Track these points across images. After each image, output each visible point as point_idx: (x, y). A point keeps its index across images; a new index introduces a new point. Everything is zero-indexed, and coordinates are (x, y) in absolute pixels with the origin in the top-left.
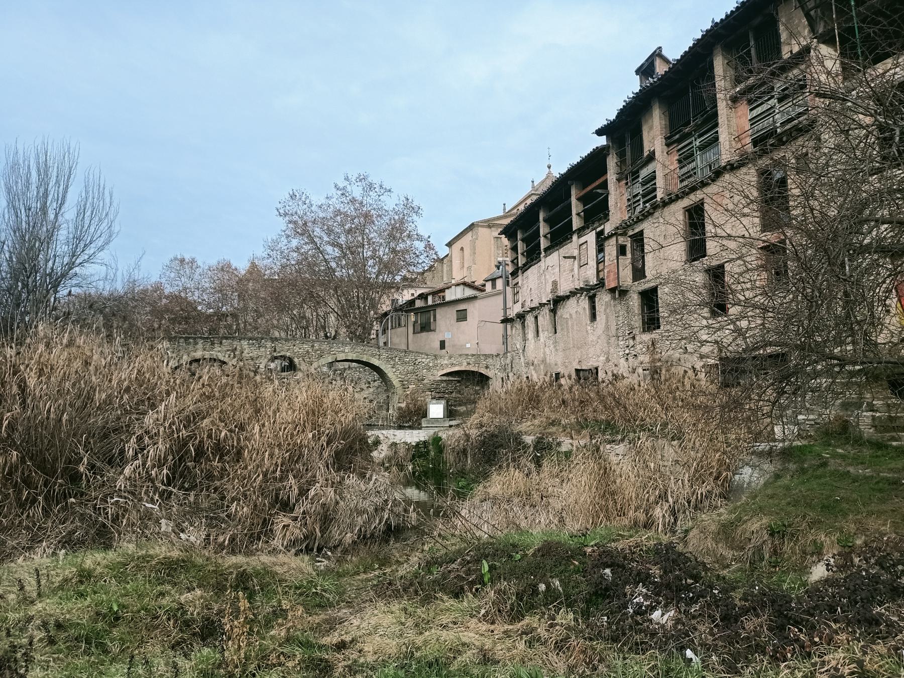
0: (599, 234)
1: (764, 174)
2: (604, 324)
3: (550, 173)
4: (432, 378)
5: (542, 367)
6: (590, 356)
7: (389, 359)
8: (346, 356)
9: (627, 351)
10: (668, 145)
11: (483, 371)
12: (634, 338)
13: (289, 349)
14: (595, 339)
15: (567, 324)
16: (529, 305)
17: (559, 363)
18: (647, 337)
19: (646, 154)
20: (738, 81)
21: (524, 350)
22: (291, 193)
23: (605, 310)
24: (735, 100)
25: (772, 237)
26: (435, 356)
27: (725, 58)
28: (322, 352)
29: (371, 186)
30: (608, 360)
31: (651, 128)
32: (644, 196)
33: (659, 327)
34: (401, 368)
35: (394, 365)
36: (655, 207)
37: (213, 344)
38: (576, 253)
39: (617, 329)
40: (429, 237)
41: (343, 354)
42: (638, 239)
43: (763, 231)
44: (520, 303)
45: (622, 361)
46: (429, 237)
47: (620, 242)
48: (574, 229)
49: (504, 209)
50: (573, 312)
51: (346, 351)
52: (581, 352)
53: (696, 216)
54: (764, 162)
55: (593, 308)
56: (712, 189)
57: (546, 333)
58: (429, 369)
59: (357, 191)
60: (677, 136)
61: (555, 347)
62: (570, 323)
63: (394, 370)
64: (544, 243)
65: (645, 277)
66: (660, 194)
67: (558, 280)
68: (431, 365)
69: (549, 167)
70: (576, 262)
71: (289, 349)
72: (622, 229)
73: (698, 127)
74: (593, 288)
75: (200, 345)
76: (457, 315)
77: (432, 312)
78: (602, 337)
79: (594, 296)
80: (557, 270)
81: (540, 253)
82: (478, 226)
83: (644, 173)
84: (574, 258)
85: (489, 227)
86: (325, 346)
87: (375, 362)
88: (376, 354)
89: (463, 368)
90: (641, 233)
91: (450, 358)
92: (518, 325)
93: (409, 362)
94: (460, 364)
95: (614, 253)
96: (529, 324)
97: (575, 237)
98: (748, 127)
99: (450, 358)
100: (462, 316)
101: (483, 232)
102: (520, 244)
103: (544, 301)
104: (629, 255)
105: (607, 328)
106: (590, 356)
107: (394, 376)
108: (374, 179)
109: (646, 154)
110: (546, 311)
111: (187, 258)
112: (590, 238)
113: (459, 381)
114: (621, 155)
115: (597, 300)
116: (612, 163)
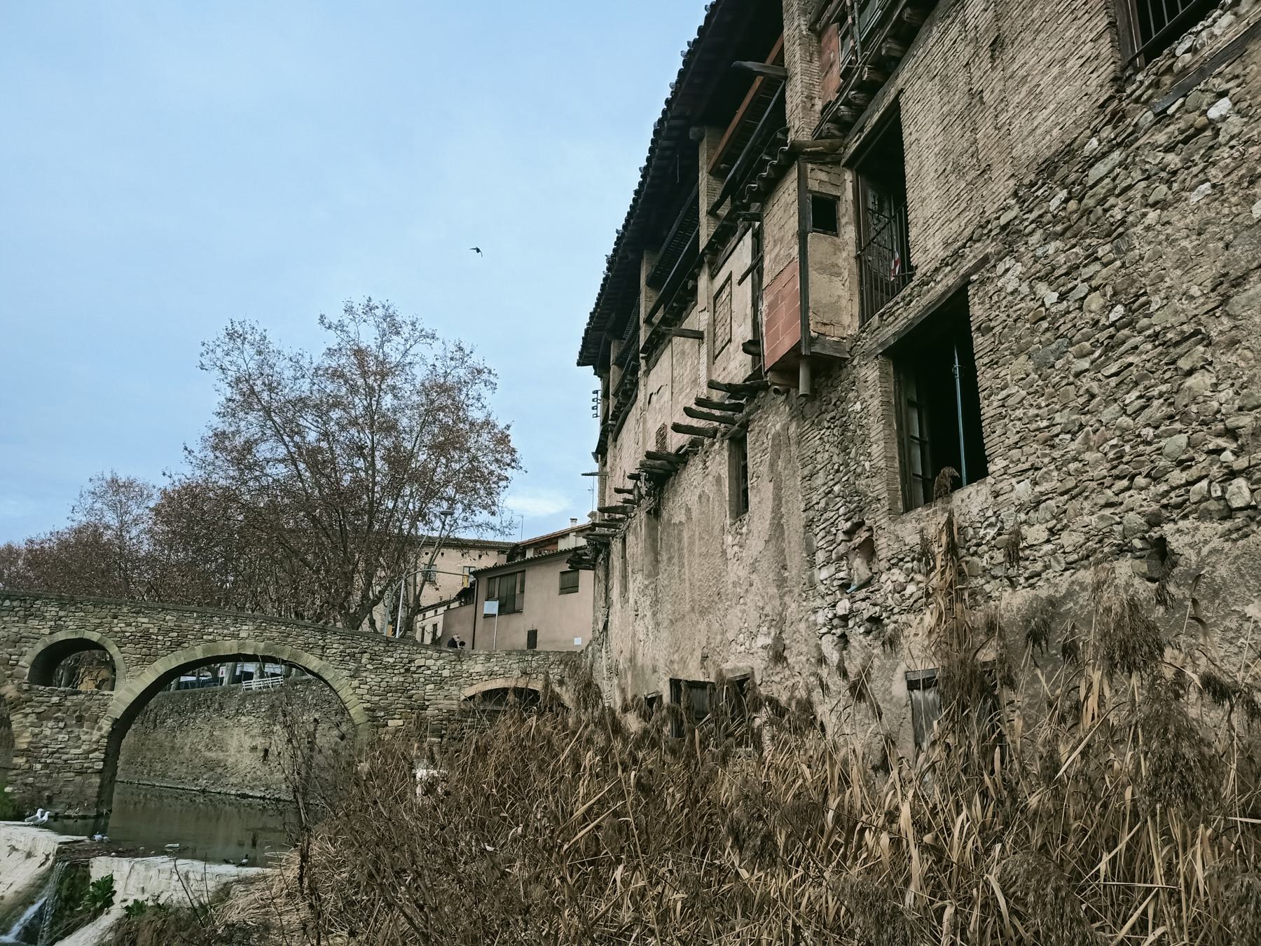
2: (768, 516)
4: (445, 704)
6: (730, 635)
7: (343, 658)
8: (241, 646)
9: (843, 606)
12: (868, 550)
13: (100, 625)
14: (743, 573)
15: (680, 541)
17: (661, 664)
23: (772, 465)
29: (392, 326)
33: (978, 471)
34: (372, 679)
35: (357, 670)
39: (809, 524)
40: (508, 427)
41: (234, 642)
46: (508, 427)
47: (813, 185)
51: (243, 634)
52: (709, 626)
55: (740, 474)
57: (640, 577)
58: (440, 683)
59: (368, 336)
61: (654, 614)
62: (686, 535)
63: (356, 683)
68: (446, 673)
71: (100, 625)
76: (562, 582)
78: (764, 565)
86: (192, 622)
88: (316, 645)
91: (488, 660)
93: (393, 666)
99: (488, 660)
104: (849, 233)
105: (778, 528)
106: (730, 635)
107: (354, 698)
111: (122, 478)
115: (750, 438)
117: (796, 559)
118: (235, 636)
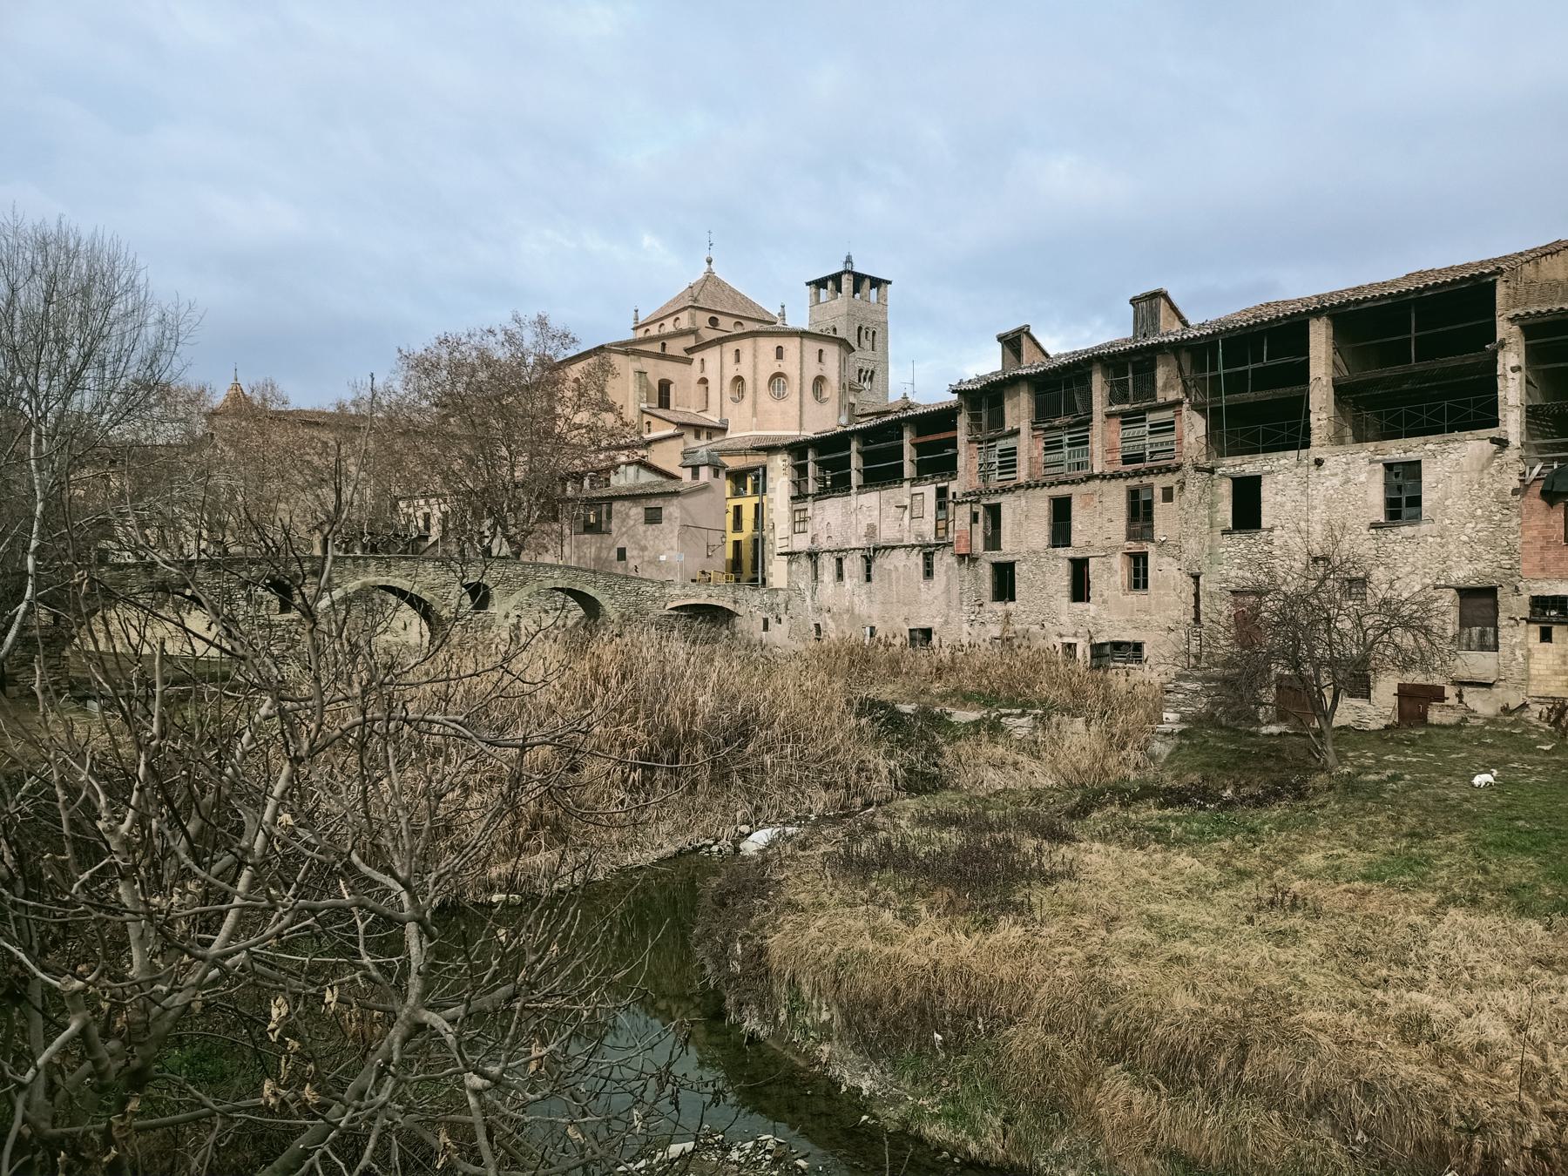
0: (942, 493)
1: (1133, 494)
3: (710, 272)
5: (846, 617)
9: (973, 617)
10: (1034, 429)
11: (730, 606)
16: (824, 544)
17: (875, 616)
18: (999, 607)
19: (1007, 429)
20: (1112, 400)
21: (814, 593)
22: (442, 338)
24: (1109, 415)
25: (1134, 547)
26: (662, 583)
27: (1103, 375)
28: (526, 577)
30: (946, 622)
31: (1017, 405)
32: (1000, 468)
36: (1018, 487)
37: (389, 566)
38: (907, 502)
42: (994, 512)
43: (1128, 540)
44: (809, 535)
45: (966, 627)
48: (906, 476)
49: (637, 319)
50: (900, 565)
53: (1061, 511)
54: (1134, 482)
56: (1083, 488)
57: (855, 580)
58: (654, 600)
60: (1046, 425)
64: (856, 479)
65: (1000, 549)
66: (1022, 475)
67: (877, 524)
69: (709, 262)
70: (907, 512)
72: (973, 496)
73: (1070, 426)
74: (930, 546)
75: (372, 568)
77: (604, 508)
79: (932, 553)
80: (877, 513)
81: (850, 488)
82: (610, 351)
83: (1003, 444)
84: (906, 507)
85: (626, 353)
87: (590, 591)
89: (701, 602)
90: (999, 505)
92: (805, 563)
94: (697, 596)
95: (968, 520)
96: (826, 564)
97: (906, 485)
98: (1119, 445)
100: (653, 517)
101: (617, 360)
102: (811, 466)
103: (854, 544)
105: (947, 590)
108: (556, 324)
109: (1007, 429)
110: (858, 554)
112: (929, 491)
113: (690, 617)
114: (975, 418)
116: (963, 421)
117: (955, 602)
118: (551, 577)
